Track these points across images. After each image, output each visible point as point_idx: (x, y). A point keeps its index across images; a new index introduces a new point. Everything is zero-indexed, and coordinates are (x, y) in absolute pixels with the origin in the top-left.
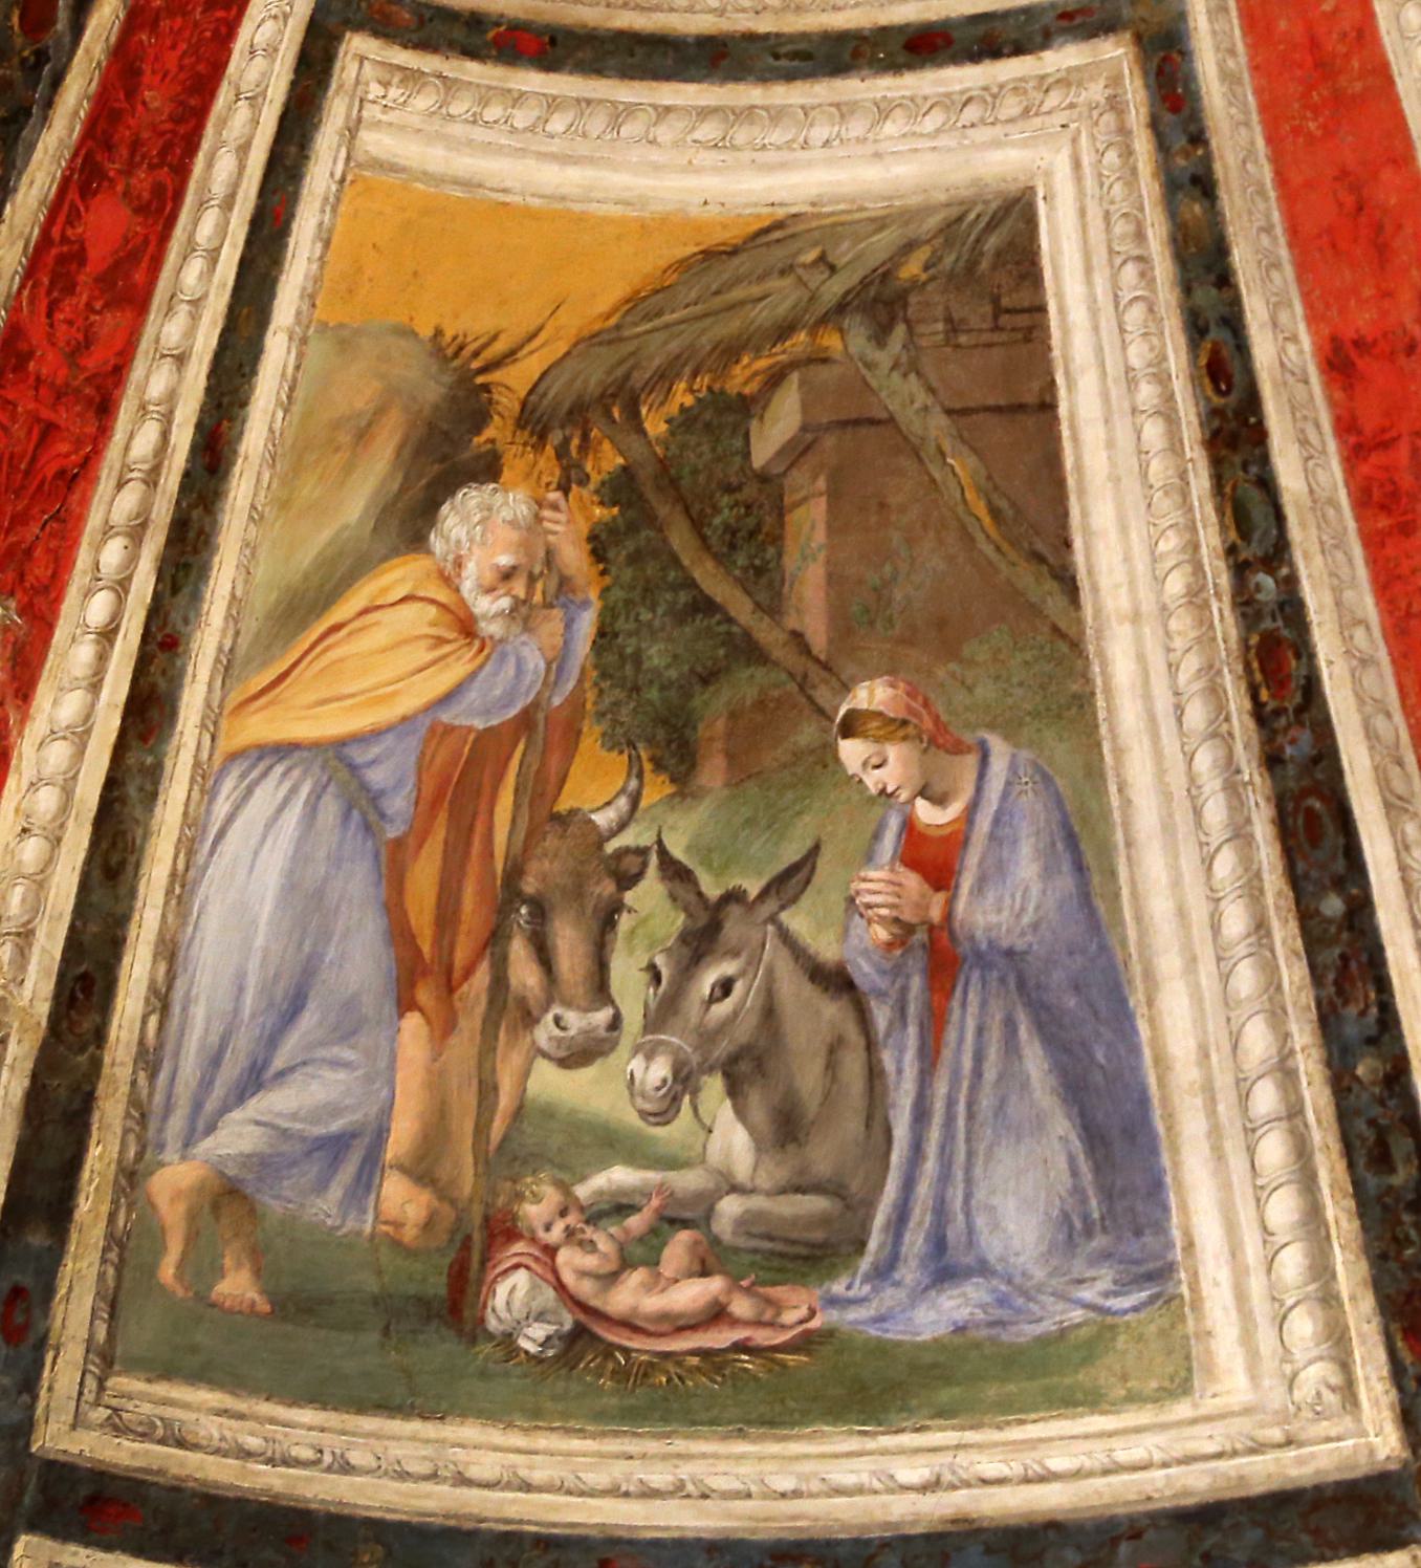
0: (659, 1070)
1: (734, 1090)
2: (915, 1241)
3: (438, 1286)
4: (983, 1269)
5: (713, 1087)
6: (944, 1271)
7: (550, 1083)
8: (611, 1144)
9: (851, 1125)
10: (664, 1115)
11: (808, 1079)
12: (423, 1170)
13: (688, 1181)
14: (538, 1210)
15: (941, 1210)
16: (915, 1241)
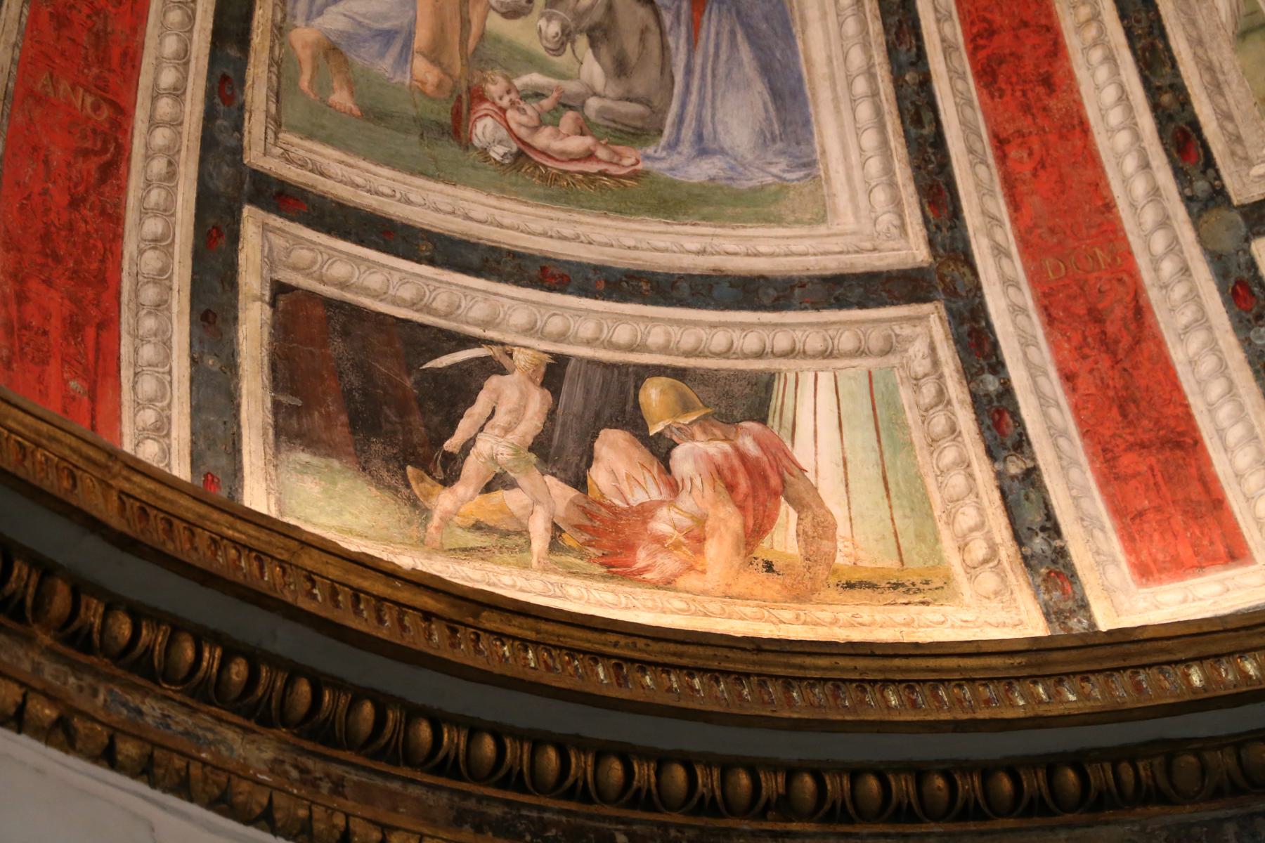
0: (554, 28)
1: (593, 44)
2: (688, 133)
3: (446, 118)
4: (722, 151)
5: (582, 42)
6: (703, 149)
7: (496, 23)
8: (531, 62)
9: (654, 72)
10: (558, 50)
11: (631, 45)
12: (434, 56)
13: (571, 87)
14: (495, 88)
15: (700, 120)
16: (688, 133)
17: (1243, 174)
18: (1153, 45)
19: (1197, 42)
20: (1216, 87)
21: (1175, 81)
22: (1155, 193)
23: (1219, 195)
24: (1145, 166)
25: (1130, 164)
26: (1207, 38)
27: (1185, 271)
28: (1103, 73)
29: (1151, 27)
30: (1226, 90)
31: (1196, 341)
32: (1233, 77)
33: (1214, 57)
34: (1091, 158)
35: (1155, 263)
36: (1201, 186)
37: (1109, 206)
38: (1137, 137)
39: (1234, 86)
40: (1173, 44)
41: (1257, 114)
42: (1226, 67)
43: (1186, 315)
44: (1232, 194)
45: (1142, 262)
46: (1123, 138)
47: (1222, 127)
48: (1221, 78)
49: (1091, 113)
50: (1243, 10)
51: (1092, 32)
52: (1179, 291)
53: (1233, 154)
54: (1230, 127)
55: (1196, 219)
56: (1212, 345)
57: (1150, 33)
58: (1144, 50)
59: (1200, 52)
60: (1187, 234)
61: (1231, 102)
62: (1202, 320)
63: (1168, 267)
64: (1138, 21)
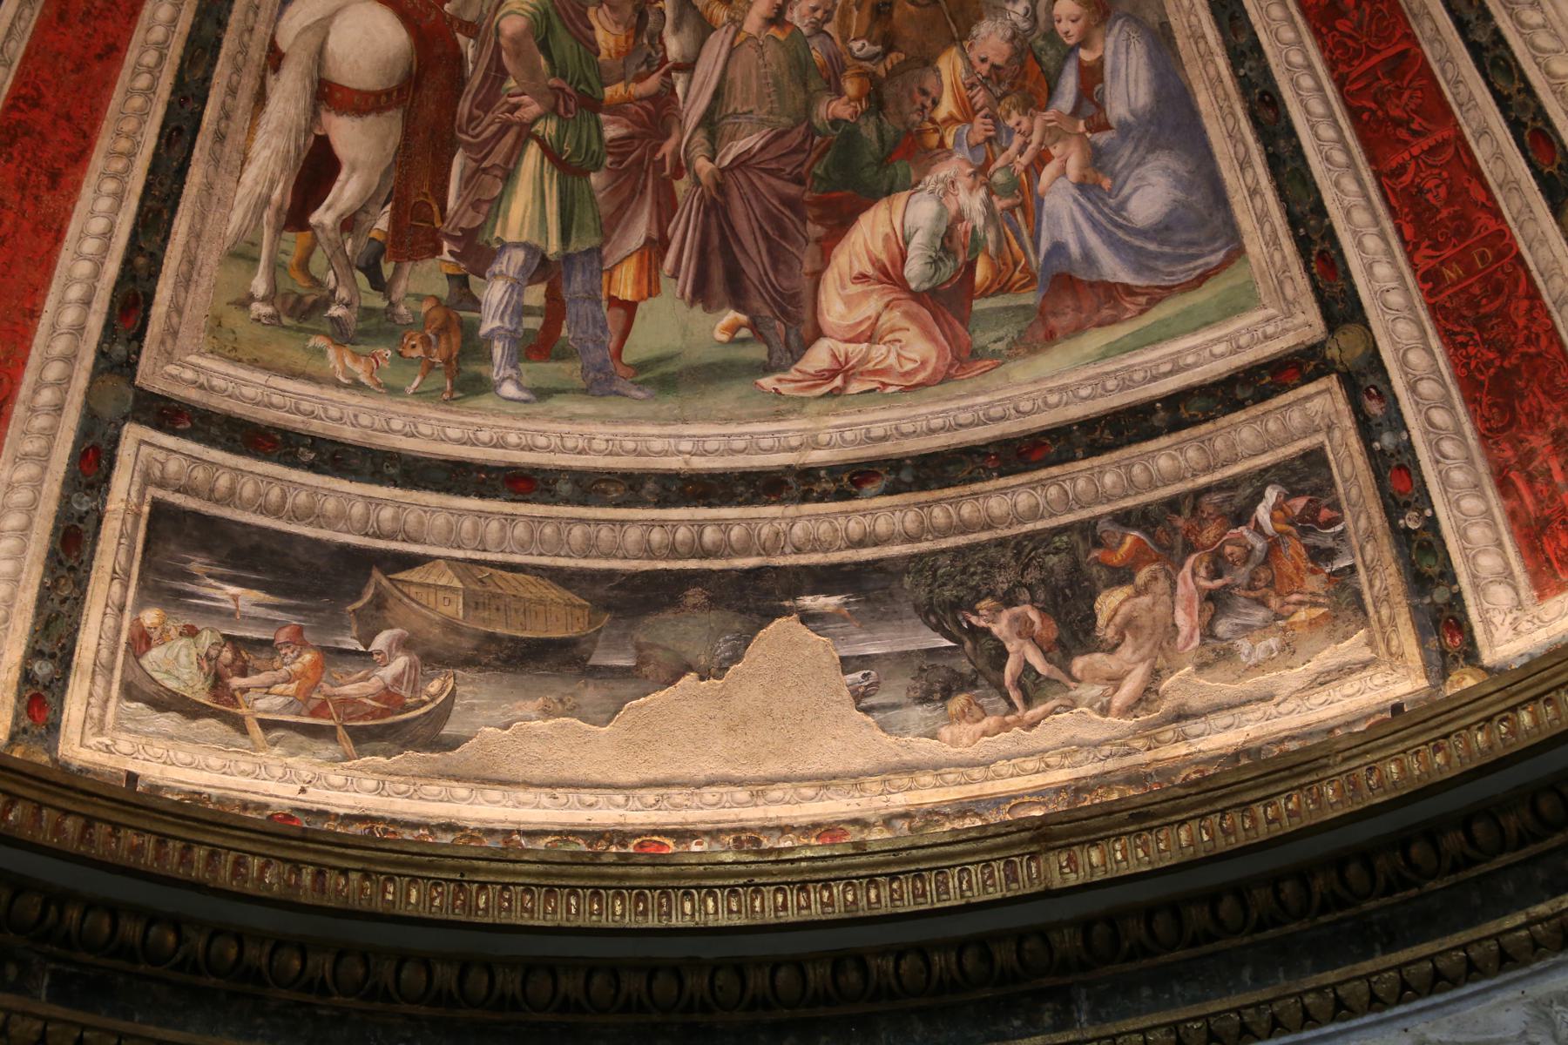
17: (160, 364)
18: (159, 213)
19: (196, 235)
20: (186, 281)
21: (158, 252)
22: (79, 329)
23: (128, 367)
24: (87, 302)
25: (75, 292)
26: (205, 238)
27: (58, 409)
28: (104, 204)
29: (168, 195)
30: (192, 288)
31: (27, 471)
32: (205, 283)
33: (201, 255)
34: (46, 265)
35: (39, 386)
36: (120, 350)
37: (34, 314)
38: (96, 274)
39: (200, 290)
40: (176, 222)
41: (203, 324)
42: (204, 271)
43: (32, 446)
44: (139, 373)
45: (29, 377)
46: (84, 268)
47: (168, 316)
48: (195, 276)
49: (73, 229)
50: (248, 236)
51: (119, 165)
52: (41, 422)
53: (163, 342)
54: (175, 320)
55: (96, 373)
56: (36, 484)
57: (164, 201)
58: (150, 210)
59: (193, 244)
60: (81, 381)
61: (190, 301)
62: (43, 458)
63: (46, 396)
64: (161, 184)
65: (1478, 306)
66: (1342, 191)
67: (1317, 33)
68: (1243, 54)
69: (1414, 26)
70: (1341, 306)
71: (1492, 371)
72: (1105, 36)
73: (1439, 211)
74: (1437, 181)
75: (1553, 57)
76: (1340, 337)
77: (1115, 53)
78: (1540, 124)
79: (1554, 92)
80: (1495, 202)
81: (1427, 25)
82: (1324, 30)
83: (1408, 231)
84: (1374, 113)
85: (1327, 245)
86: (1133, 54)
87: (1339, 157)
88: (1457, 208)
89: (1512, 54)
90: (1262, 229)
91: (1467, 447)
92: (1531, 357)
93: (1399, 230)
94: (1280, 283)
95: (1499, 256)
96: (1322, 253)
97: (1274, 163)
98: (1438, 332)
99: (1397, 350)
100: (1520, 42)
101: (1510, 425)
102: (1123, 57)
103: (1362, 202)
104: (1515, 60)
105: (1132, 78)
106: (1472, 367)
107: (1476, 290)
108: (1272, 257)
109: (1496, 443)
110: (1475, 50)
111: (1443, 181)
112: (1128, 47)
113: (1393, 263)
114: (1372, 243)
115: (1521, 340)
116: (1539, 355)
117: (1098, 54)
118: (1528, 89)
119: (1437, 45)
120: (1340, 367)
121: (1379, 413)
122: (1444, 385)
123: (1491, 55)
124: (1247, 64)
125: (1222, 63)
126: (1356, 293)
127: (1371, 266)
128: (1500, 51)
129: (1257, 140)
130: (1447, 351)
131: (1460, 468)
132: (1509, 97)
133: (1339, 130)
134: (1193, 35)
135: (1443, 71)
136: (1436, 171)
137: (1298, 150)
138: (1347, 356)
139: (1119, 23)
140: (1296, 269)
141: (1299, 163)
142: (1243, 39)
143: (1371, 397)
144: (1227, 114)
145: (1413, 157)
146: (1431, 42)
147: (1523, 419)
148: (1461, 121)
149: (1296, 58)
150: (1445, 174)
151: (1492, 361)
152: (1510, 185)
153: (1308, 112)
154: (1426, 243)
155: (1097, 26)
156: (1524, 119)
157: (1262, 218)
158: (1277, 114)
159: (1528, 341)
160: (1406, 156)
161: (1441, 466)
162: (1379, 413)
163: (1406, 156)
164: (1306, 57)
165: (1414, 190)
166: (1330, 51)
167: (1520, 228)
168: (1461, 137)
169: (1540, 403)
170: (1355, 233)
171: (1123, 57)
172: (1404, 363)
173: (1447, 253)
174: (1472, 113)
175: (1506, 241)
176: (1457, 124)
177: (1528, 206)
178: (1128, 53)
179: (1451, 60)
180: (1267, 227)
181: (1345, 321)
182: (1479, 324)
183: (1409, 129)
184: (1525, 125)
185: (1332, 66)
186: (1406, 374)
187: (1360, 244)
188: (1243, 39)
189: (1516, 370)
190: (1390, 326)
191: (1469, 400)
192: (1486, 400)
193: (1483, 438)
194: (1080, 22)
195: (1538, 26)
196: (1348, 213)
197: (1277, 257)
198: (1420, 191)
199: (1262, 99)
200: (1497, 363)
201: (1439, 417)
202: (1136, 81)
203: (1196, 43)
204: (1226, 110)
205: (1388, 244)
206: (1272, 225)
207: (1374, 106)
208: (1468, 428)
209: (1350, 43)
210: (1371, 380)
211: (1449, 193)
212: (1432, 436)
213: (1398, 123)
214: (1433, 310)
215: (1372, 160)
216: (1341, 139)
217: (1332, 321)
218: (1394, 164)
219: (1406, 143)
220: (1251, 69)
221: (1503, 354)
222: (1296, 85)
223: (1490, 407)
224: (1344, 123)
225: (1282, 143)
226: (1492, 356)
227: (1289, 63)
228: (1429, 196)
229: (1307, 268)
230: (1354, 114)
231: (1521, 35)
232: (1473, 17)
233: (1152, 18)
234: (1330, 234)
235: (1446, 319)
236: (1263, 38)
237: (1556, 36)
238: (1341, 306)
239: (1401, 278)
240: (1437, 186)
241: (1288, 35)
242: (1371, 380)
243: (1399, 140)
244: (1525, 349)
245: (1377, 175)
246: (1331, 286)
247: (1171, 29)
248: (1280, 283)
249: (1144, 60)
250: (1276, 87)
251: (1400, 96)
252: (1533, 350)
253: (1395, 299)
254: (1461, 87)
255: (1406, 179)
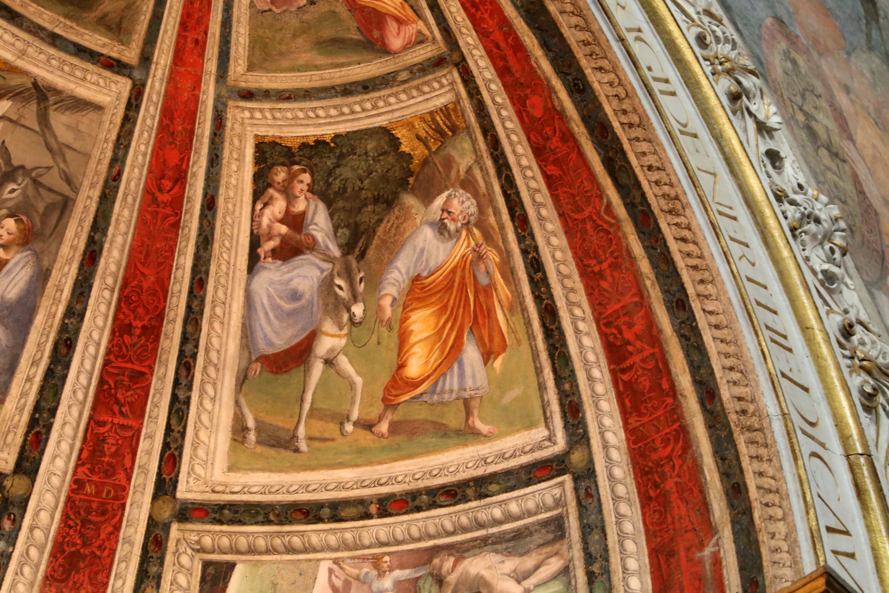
65: (89, 513)
66: (70, 412)
67: (113, 332)
68: (74, 313)
69: (156, 365)
70: (28, 464)
71: (73, 549)
72: (17, 252)
73: (105, 456)
74: (114, 442)
75: (203, 428)
76: (17, 478)
77: (16, 264)
78: (176, 453)
79: (193, 445)
80: (132, 472)
81: (162, 370)
82: (117, 334)
83: (85, 454)
84: (110, 388)
85: (43, 431)
86: (23, 272)
87: (80, 395)
88: (114, 461)
89: (188, 413)
90: (19, 400)
91: (36, 576)
92: (96, 556)
93: (81, 450)
94: (9, 431)
95: (116, 498)
96: (38, 433)
97: (49, 373)
98: (63, 511)
99: (38, 505)
100: (195, 411)
101: (63, 581)
102: (18, 269)
103: (75, 424)
104: (187, 417)
105: (14, 281)
106: (67, 539)
107: (94, 506)
108: (14, 416)
109: (50, 585)
110: (174, 398)
111: (117, 444)
112: (24, 266)
113: (67, 464)
114: (65, 446)
115: (97, 544)
116: (100, 558)
117: (8, 258)
118: (183, 434)
119: (160, 382)
120: (6, 493)
121: (7, 529)
122: (47, 539)
123: (179, 406)
124: (72, 320)
125: (61, 310)
126: (40, 464)
127: (56, 457)
128: (184, 407)
129: (50, 357)
130: (60, 524)
131: (25, 585)
132: (173, 431)
133: (89, 384)
134: (57, 286)
135: (154, 396)
136: (118, 437)
137: (64, 377)
138: (13, 490)
139: (29, 252)
140: (21, 431)
141: (60, 383)
142: (79, 307)
143: (9, 518)
144: (45, 334)
145: (112, 422)
146: (159, 379)
147: (71, 583)
148: (145, 424)
149: (96, 336)
150: (120, 442)
151: (77, 544)
152: (145, 470)
153: (82, 364)
154: (89, 466)
155: (18, 245)
156: (172, 446)
157: (24, 394)
158: (68, 353)
159: (99, 547)
160: (110, 419)
161: (17, 577)
162: (7, 529)
163: (110, 419)
164: (100, 339)
165: (101, 438)
166: (113, 346)
167: (134, 493)
168: (139, 431)
169: (83, 581)
170: (60, 436)
171: (18, 269)
172: (37, 514)
173: (95, 478)
174: (152, 424)
175: (124, 493)
176: (142, 424)
177: (145, 485)
178: (22, 269)
179: (161, 394)
180: (23, 401)
181: (25, 473)
182: (85, 522)
183: (120, 409)
184: (170, 449)
185: (108, 352)
186: (34, 520)
187: (59, 443)
188: (79, 307)
189: (84, 557)
190: (44, 491)
191: (53, 555)
192: (60, 561)
193: (46, 578)
194: (11, 237)
195: (207, 410)
196: (64, 424)
197: (17, 418)
198: (104, 440)
199: (66, 341)
200: (78, 547)
201: (33, 552)
202: (16, 284)
203: (57, 291)
204: (46, 332)
205: (71, 453)
206: (26, 401)
207: (113, 385)
208: (43, 568)
209: (124, 349)
210: (15, 511)
211: (115, 452)
212: (23, 559)
213: (117, 402)
214: (69, 499)
215: (94, 409)
216: (87, 388)
217: (19, 468)
218: (101, 419)
219: (114, 413)
220: (72, 323)
221: (84, 545)
222: (86, 347)
223: (60, 565)
224: (94, 382)
225: (60, 368)
226: (79, 542)
227: (91, 335)
228: (106, 446)
229: (26, 434)
230: (102, 382)
231: (198, 408)
232: (184, 383)
233: (46, 263)
234: (49, 427)
235: (71, 508)
236: (88, 314)
237: (211, 421)
238: (28, 464)
239: (65, 473)
240: (113, 444)
241: (100, 322)
242: (15, 511)
243: (112, 410)
244: (95, 550)
245: (91, 418)
246: (31, 452)
247: (50, 275)
248: (9, 431)
249: (27, 278)
250: (76, 341)
251: (127, 391)
252: (98, 553)
253: (55, 481)
254: (156, 409)
255: (102, 430)
